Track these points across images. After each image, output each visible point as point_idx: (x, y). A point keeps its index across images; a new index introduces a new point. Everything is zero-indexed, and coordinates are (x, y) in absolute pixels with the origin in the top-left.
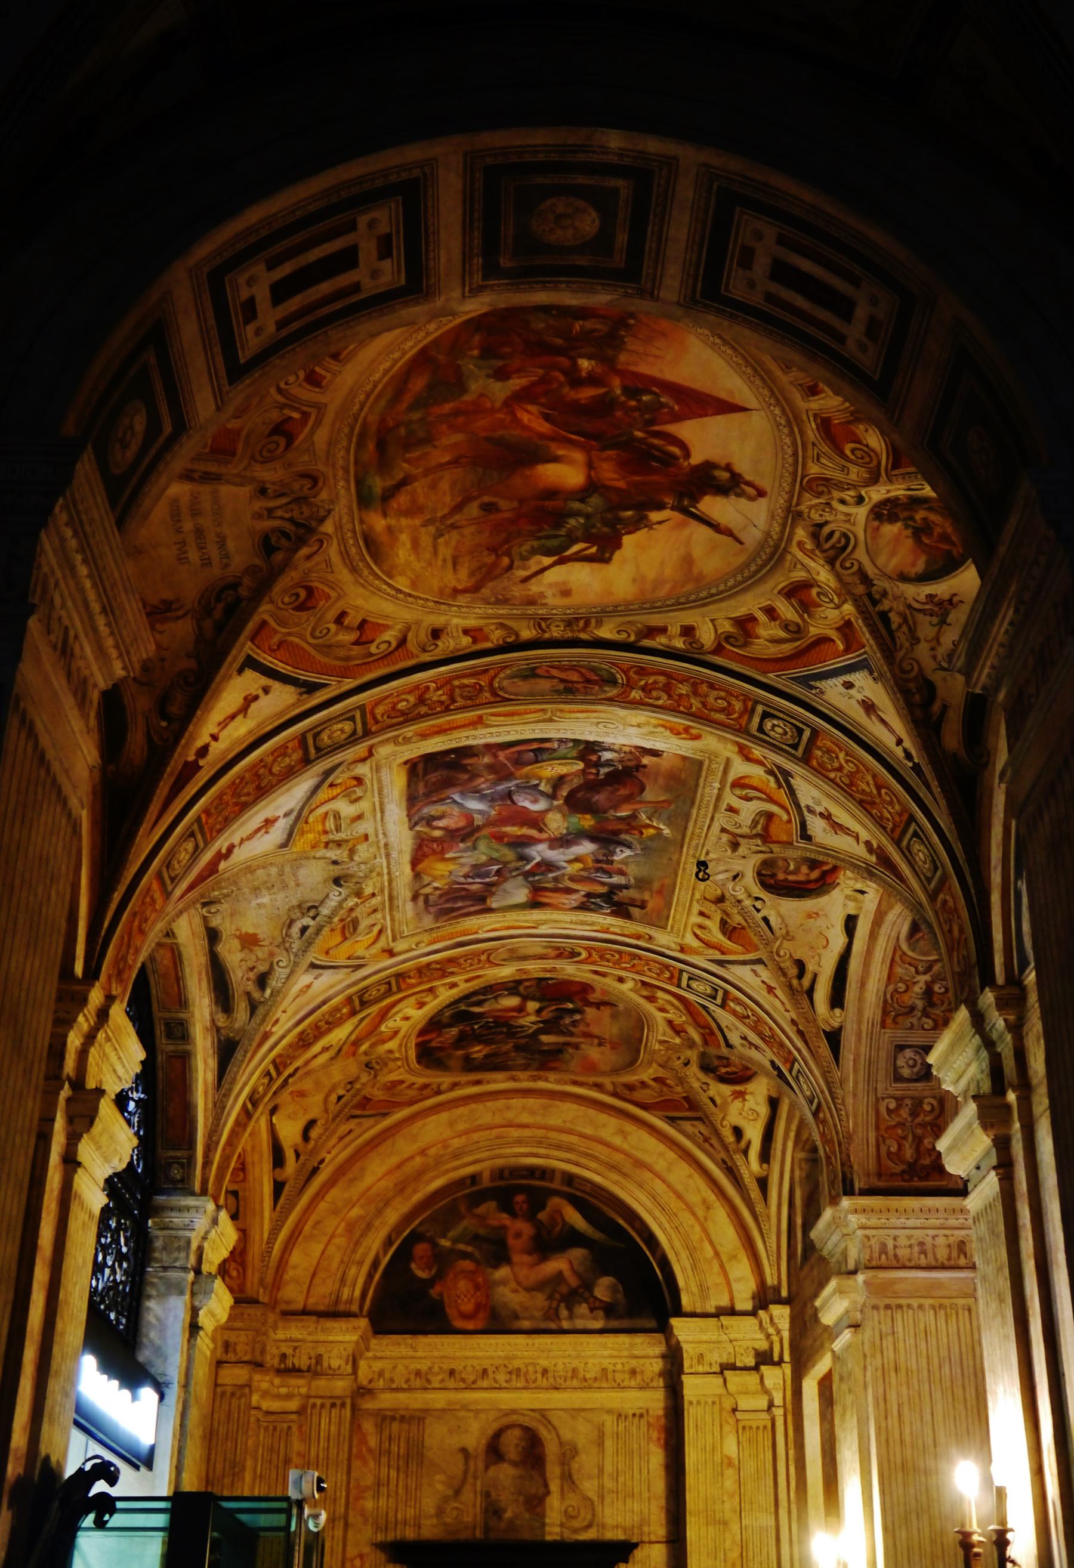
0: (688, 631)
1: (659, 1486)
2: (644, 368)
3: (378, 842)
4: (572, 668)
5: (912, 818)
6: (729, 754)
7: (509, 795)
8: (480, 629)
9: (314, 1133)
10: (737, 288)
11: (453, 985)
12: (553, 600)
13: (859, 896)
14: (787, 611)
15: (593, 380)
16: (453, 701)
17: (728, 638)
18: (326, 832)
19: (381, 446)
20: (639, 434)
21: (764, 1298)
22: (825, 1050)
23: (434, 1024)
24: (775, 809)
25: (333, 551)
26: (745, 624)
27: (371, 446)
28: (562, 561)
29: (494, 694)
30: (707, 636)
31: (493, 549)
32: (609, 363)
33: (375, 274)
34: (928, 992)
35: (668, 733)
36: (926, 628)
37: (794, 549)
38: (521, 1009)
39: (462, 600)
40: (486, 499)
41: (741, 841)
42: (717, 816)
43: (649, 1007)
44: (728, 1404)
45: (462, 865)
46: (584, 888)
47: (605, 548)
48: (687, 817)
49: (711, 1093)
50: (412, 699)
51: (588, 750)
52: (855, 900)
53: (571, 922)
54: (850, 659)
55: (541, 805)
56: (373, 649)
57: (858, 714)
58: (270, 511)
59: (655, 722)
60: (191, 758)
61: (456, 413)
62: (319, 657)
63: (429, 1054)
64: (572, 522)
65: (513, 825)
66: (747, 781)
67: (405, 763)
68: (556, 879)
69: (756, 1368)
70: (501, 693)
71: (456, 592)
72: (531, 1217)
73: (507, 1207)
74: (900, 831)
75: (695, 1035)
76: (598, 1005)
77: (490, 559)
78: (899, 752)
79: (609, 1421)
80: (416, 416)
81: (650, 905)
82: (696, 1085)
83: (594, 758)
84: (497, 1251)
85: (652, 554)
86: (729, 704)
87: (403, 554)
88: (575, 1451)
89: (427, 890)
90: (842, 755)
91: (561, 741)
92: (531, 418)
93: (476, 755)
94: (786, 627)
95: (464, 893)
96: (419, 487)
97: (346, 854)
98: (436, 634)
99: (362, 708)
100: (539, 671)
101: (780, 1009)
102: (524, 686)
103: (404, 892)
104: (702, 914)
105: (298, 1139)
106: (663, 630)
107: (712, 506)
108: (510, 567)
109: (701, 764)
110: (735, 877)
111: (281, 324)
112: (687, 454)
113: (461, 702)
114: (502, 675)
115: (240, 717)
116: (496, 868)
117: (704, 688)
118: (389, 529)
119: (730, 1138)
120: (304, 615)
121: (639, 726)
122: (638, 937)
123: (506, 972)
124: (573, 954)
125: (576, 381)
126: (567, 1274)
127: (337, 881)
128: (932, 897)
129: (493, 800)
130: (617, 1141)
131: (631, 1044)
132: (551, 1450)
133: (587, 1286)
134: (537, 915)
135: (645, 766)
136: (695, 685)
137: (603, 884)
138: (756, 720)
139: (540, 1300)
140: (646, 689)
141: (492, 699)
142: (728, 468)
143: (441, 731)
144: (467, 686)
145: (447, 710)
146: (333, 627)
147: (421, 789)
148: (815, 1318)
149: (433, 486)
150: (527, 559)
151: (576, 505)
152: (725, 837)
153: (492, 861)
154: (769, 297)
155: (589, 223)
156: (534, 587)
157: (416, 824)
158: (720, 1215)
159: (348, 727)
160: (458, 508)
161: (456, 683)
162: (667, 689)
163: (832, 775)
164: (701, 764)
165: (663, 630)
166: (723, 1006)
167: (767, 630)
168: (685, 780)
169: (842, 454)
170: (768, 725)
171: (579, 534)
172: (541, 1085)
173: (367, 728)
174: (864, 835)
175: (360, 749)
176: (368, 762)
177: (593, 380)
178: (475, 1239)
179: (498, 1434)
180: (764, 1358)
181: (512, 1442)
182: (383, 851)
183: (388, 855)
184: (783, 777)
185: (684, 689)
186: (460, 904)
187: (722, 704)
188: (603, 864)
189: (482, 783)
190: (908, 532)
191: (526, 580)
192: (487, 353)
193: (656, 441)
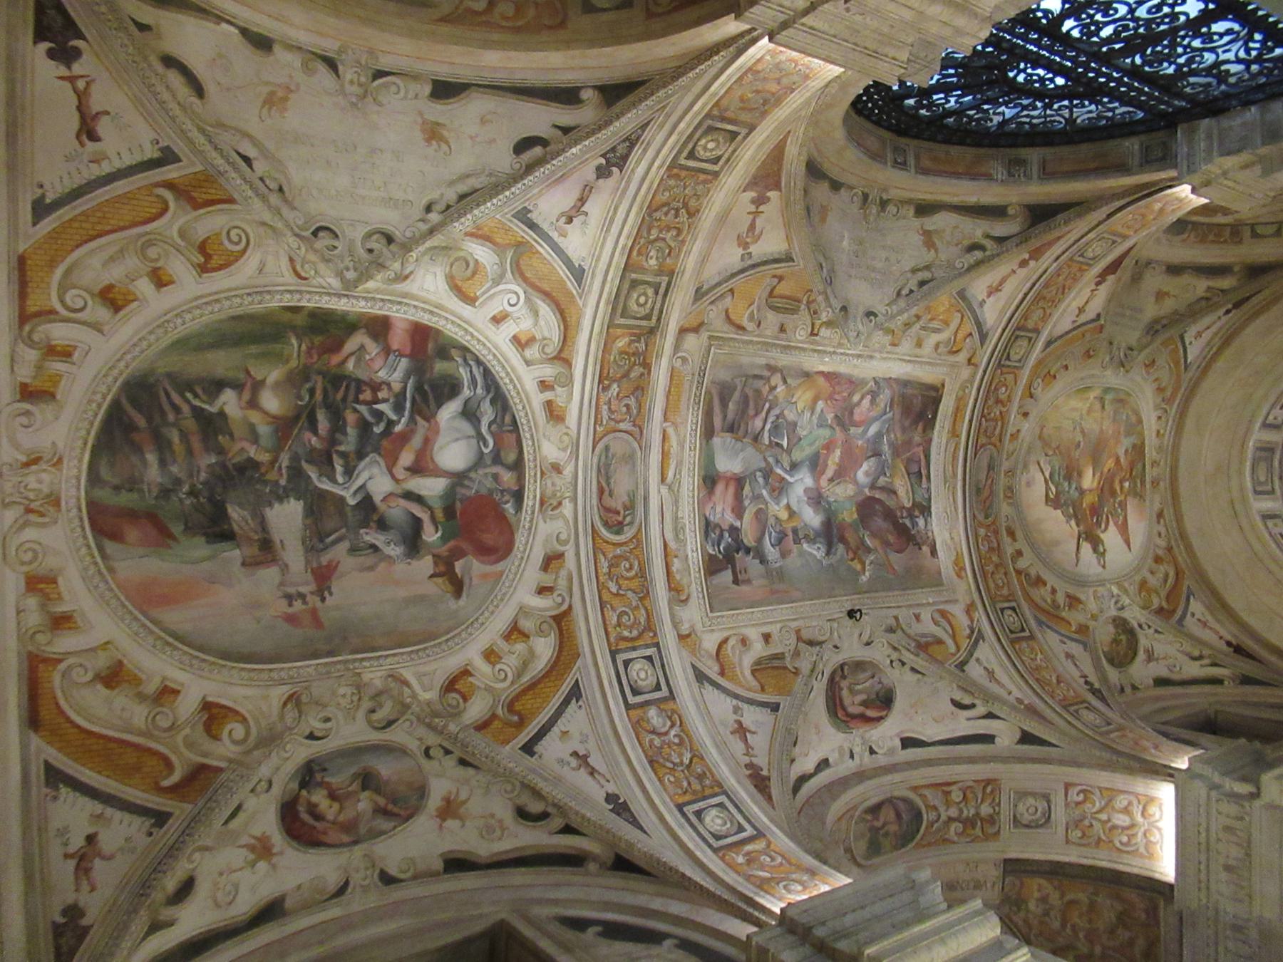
0: (1019, 553)
7: (877, 454)
8: (1017, 438)
9: (174, 78)
11: (544, 385)
12: (1024, 478)
13: (848, 755)
14: (1060, 598)
15: (1122, 488)
17: (1027, 575)
18: (932, 319)
19: (1121, 401)
24: (950, 642)
30: (1022, 563)
31: (1058, 447)
37: (1091, 590)
41: (899, 632)
45: (800, 414)
47: (1054, 502)
48: (890, 589)
49: (251, 803)
50: (1002, 397)
51: (924, 509)
52: (841, 755)
53: (676, 519)
60: (1032, 263)
64: (1066, 484)
65: (841, 458)
67: (943, 385)
68: (757, 498)
71: (1042, 428)
77: (1053, 445)
81: (744, 588)
82: (264, 771)
83: (917, 513)
85: (1056, 526)
89: (776, 379)
90: (1039, 656)
91: (928, 490)
93: (924, 431)
94: (1054, 601)
95: (751, 412)
96: (1097, 415)
97: (892, 327)
102: (984, 463)
103: (783, 360)
104: (767, 637)
105: (172, 46)
106: (1015, 540)
107: (1086, 548)
109: (942, 585)
110: (836, 647)
114: (994, 450)
116: (785, 444)
117: (1003, 571)
122: (674, 588)
125: (1121, 482)
127: (844, 309)
134: (689, 484)
137: (760, 540)
138: (1006, 605)
143: (958, 411)
145: (983, 416)
147: (909, 391)
152: (892, 622)
153: (795, 441)
156: (1033, 469)
157: (876, 382)
160: (1082, 431)
162: (991, 549)
164: (942, 585)
165: (1015, 540)
170: (1010, 612)
177: (1122, 488)
183: (859, 356)
185: (995, 558)
186: (731, 406)
189: (898, 436)
192: (1134, 446)
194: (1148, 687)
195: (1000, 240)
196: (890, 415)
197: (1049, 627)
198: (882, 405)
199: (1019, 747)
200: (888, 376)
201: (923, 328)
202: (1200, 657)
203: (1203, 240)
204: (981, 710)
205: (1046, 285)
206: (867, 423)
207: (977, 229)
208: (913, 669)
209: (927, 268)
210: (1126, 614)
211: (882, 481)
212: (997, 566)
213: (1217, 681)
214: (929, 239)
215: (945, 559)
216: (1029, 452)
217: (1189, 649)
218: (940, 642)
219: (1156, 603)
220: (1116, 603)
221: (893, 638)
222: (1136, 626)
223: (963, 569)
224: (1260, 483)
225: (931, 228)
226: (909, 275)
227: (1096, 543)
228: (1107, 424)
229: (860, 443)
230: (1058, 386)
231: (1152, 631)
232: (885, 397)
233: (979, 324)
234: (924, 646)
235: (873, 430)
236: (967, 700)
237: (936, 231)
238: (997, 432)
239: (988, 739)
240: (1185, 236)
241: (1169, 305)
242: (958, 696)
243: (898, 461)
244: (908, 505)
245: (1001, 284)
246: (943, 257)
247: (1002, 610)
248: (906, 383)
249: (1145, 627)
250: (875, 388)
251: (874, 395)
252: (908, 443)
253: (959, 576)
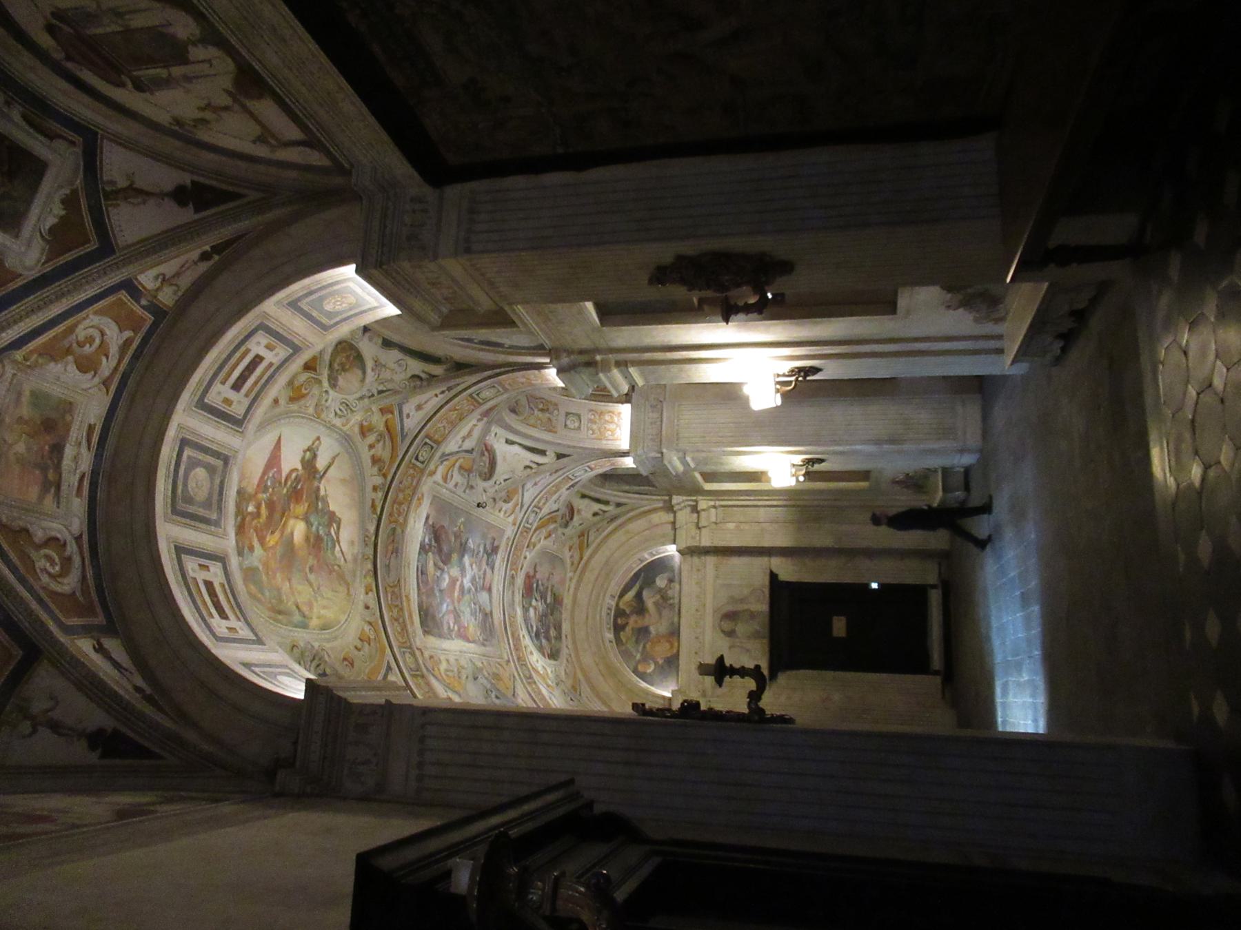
0: (375, 489)
1: (744, 560)
5: (471, 395)
7: (441, 591)
10: (238, 409)
14: (371, 438)
15: (258, 507)
19: (280, 612)
21: (670, 508)
22: (565, 460)
23: (541, 649)
24: (457, 465)
25: (327, 645)
26: (375, 460)
27: (280, 617)
30: (378, 480)
31: (330, 572)
32: (252, 497)
33: (216, 575)
34: (542, 410)
36: (386, 375)
37: (345, 429)
38: (535, 609)
39: (352, 591)
43: (538, 547)
44: (714, 526)
46: (484, 566)
47: (332, 519)
51: (423, 549)
54: (396, 413)
55: (446, 576)
57: (421, 413)
61: (267, 574)
63: (553, 655)
69: (698, 512)
72: (628, 616)
73: (623, 627)
74: (475, 402)
75: (552, 526)
76: (535, 571)
78: (441, 396)
79: (720, 581)
80: (267, 594)
84: (643, 632)
85: (337, 495)
88: (732, 598)
92: (272, 540)
94: (379, 441)
98: (367, 607)
99: (400, 647)
101: (545, 479)
102: (393, 573)
106: (373, 501)
107: (321, 464)
111: (239, 619)
112: (296, 470)
118: (318, 618)
119: (598, 518)
123: (519, 611)
124: (513, 577)
125: (258, 515)
126: (653, 600)
127: (476, 679)
128: (506, 390)
130: (596, 572)
131: (554, 559)
132: (731, 608)
133: (660, 590)
139: (666, 613)
140: (399, 514)
142: (305, 452)
143: (411, 616)
145: (401, 609)
147: (436, 630)
148: (677, 475)
149: (300, 593)
154: (247, 395)
155: (200, 472)
156: (349, 557)
158: (633, 526)
159: (407, 655)
162: (401, 504)
166: (540, 509)
168: (441, 506)
170: (421, 458)
172: (569, 607)
173: (408, 647)
174: (474, 422)
175: (418, 653)
177: (258, 507)
178: (637, 642)
179: (723, 631)
180: (695, 509)
181: (727, 625)
184: (445, 457)
185: (401, 496)
188: (474, 554)
197: (402, 429)
206: (448, 612)
211: (438, 574)
212: (403, 491)
224: (211, 470)
227: (309, 464)
228: (286, 587)
252: (428, 596)
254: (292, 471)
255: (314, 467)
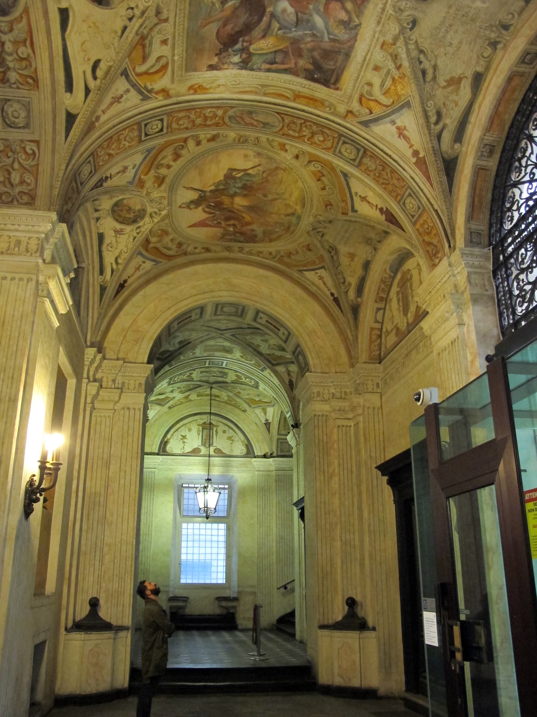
2: (215, 230)
3: (381, 31)
4: (247, 124)
6: (174, 86)
7: (298, 22)
8: (281, 149)
14: (163, 171)
15: (229, 225)
16: (301, 124)
18: (393, 79)
19: (289, 228)
20: (218, 213)
27: (291, 229)
28: (245, 170)
29: (283, 119)
30: (191, 144)
31: (267, 181)
32: (225, 229)
35: (204, 85)
39: (283, 166)
40: (265, 199)
41: (156, 21)
42: (172, 30)
47: (229, 176)
48: (190, 19)
56: (320, 168)
58: (325, 228)
59: (211, 91)
62: (337, 184)
66: (161, 74)
67: (337, 89)
70: (280, 119)
71: (285, 170)
77: (269, 178)
80: (277, 230)
86: (178, 124)
87: (296, 194)
91: (260, 69)
92: (247, 218)
94: (162, 165)
96: (283, 212)
97: (398, 44)
98: (297, 157)
100: (262, 125)
102: (270, 120)
106: (209, 140)
107: (194, 196)
108: (264, 172)
109: (187, 71)
112: (203, 209)
113: (299, 122)
114: (278, 129)
115: (368, 199)
117: (190, 126)
118: (296, 204)
120: (332, 201)
121: (219, 86)
125: (234, 225)
129: (308, 21)
135: (217, 55)
136: (194, 125)
140: (215, 116)
141: (285, 117)
142: (191, 209)
143: (313, 101)
144: (294, 131)
145: (306, 121)
146: (327, 188)
147: (341, 58)
150: (257, 174)
151: (238, 191)
152: (164, 16)
156: (257, 161)
157: (357, 26)
160: (275, 200)
161: (297, 135)
162: (206, 118)
163: (127, 130)
165: (209, 140)
167: (169, 160)
169: (160, 230)
170: (160, 126)
171: (238, 181)
176: (350, 109)
182: (382, 21)
183: (383, 9)
185: (199, 121)
187: (181, 122)
190: (133, 208)
191: (259, 165)
192: (256, 236)
193: (213, 211)
194: (97, 228)
195: (439, 137)
196: (326, 39)
197: (145, 158)
198: (336, 31)
199: (64, 112)
200: (359, 37)
201: (388, 72)
202: (117, 263)
203: (383, 281)
204: (92, 84)
205: (393, 171)
207: (451, 122)
208: (125, 28)
209: (434, 78)
210: (147, 219)
211: (276, 25)
212: (193, 121)
213: (102, 272)
214: (455, 82)
215: (204, 76)
216: (270, 158)
217: (122, 257)
218: (145, 58)
219: (153, 240)
220: (156, 213)
221: (151, 13)
222: (141, 224)
223: (196, 92)
224: (222, 308)
225: (462, 85)
226: (433, 63)
227: (196, 203)
229: (311, 7)
230: (311, 182)
231: (135, 235)
232: (342, 34)
233: (376, 120)
234: (142, 42)
235: (318, 21)
236: (99, 73)
237: (458, 88)
238: (291, 132)
239: (69, 87)
240: (388, 271)
241: (344, 260)
242: (103, 66)
243: (287, 44)
244: (252, 48)
245: (406, 138)
246: (439, 92)
247: (162, 120)
248: (348, 55)
249: (138, 230)
250: (352, 25)
251: (345, 24)
253: (190, 88)
254: (205, 211)
255: (198, 199)
